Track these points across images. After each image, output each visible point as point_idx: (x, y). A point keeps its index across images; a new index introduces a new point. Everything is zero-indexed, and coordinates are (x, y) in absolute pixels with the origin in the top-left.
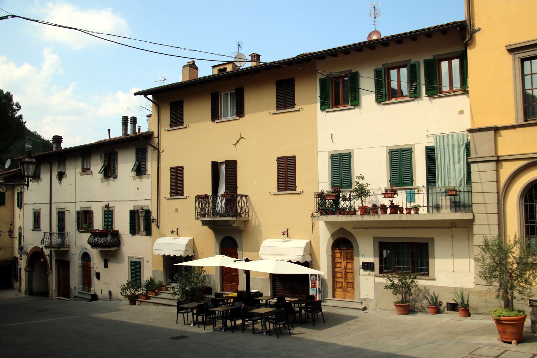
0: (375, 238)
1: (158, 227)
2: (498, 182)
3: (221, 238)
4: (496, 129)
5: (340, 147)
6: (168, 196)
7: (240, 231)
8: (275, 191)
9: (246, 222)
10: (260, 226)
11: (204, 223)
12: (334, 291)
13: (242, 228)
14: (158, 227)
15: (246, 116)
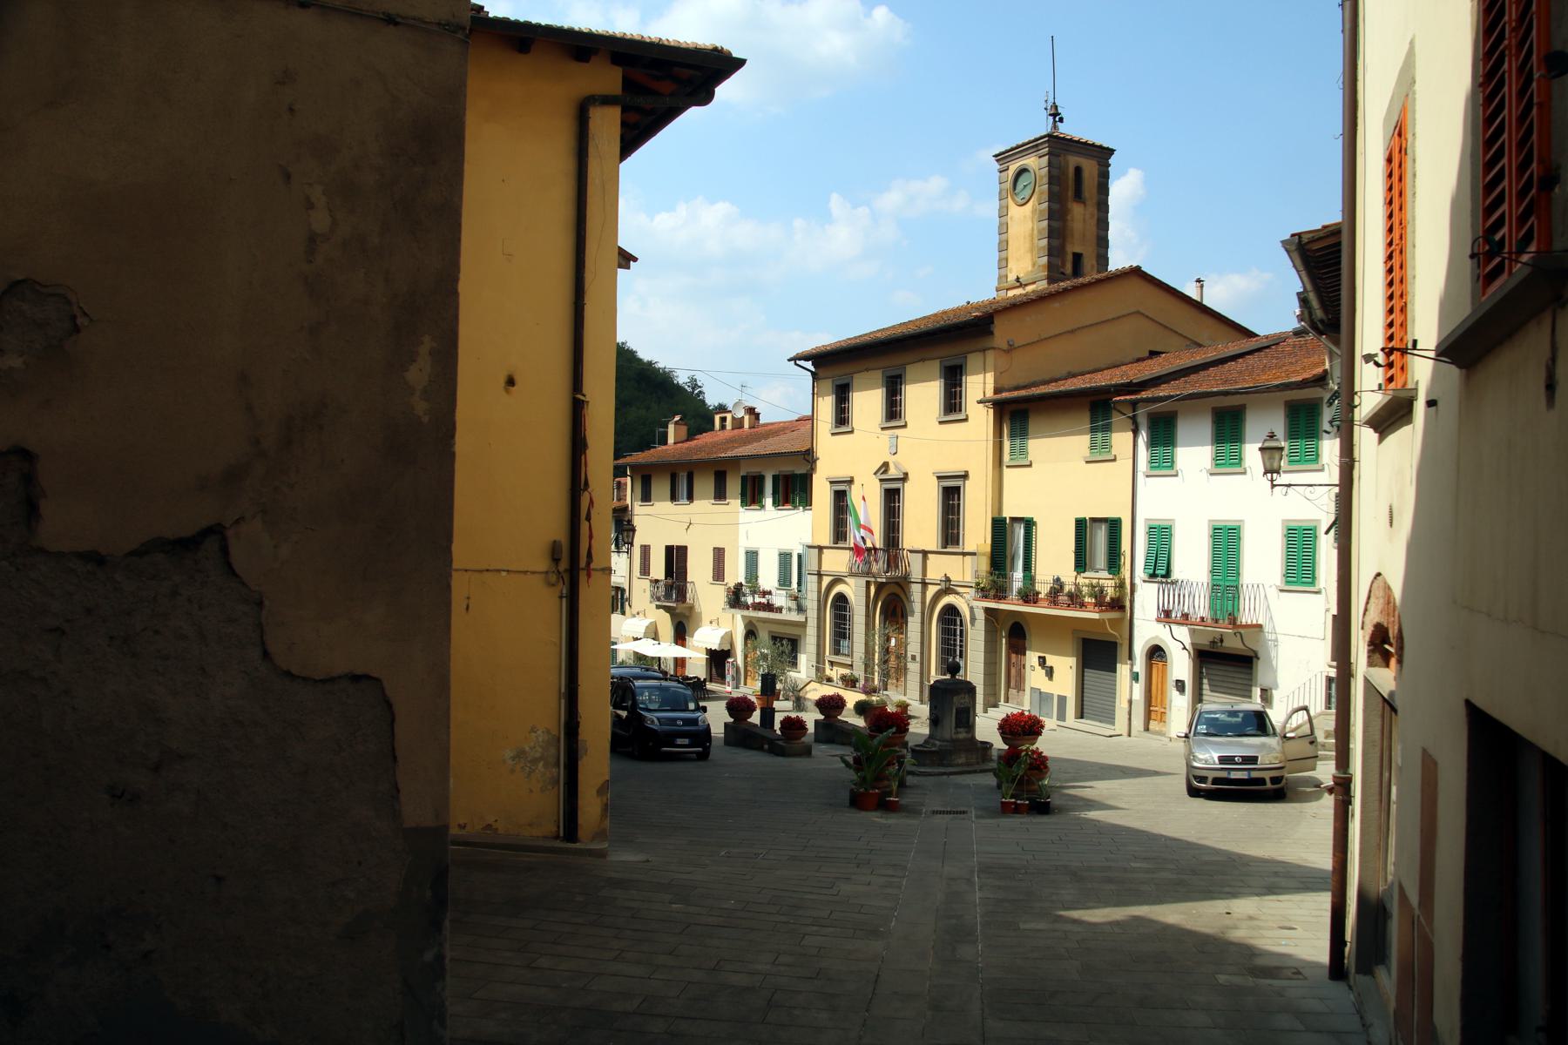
0: (770, 632)
1: (630, 606)
2: (819, 591)
3: (676, 622)
4: (821, 549)
5: (752, 545)
6: (638, 575)
7: (688, 618)
8: (711, 580)
9: (691, 608)
10: (701, 613)
11: (658, 607)
12: (746, 679)
13: (687, 614)
14: (630, 606)
15: (695, 502)
